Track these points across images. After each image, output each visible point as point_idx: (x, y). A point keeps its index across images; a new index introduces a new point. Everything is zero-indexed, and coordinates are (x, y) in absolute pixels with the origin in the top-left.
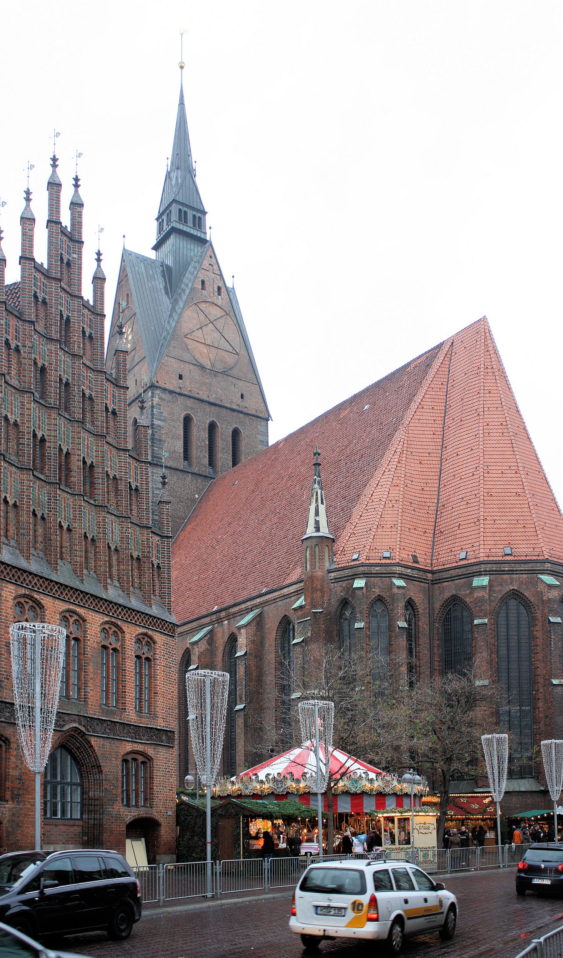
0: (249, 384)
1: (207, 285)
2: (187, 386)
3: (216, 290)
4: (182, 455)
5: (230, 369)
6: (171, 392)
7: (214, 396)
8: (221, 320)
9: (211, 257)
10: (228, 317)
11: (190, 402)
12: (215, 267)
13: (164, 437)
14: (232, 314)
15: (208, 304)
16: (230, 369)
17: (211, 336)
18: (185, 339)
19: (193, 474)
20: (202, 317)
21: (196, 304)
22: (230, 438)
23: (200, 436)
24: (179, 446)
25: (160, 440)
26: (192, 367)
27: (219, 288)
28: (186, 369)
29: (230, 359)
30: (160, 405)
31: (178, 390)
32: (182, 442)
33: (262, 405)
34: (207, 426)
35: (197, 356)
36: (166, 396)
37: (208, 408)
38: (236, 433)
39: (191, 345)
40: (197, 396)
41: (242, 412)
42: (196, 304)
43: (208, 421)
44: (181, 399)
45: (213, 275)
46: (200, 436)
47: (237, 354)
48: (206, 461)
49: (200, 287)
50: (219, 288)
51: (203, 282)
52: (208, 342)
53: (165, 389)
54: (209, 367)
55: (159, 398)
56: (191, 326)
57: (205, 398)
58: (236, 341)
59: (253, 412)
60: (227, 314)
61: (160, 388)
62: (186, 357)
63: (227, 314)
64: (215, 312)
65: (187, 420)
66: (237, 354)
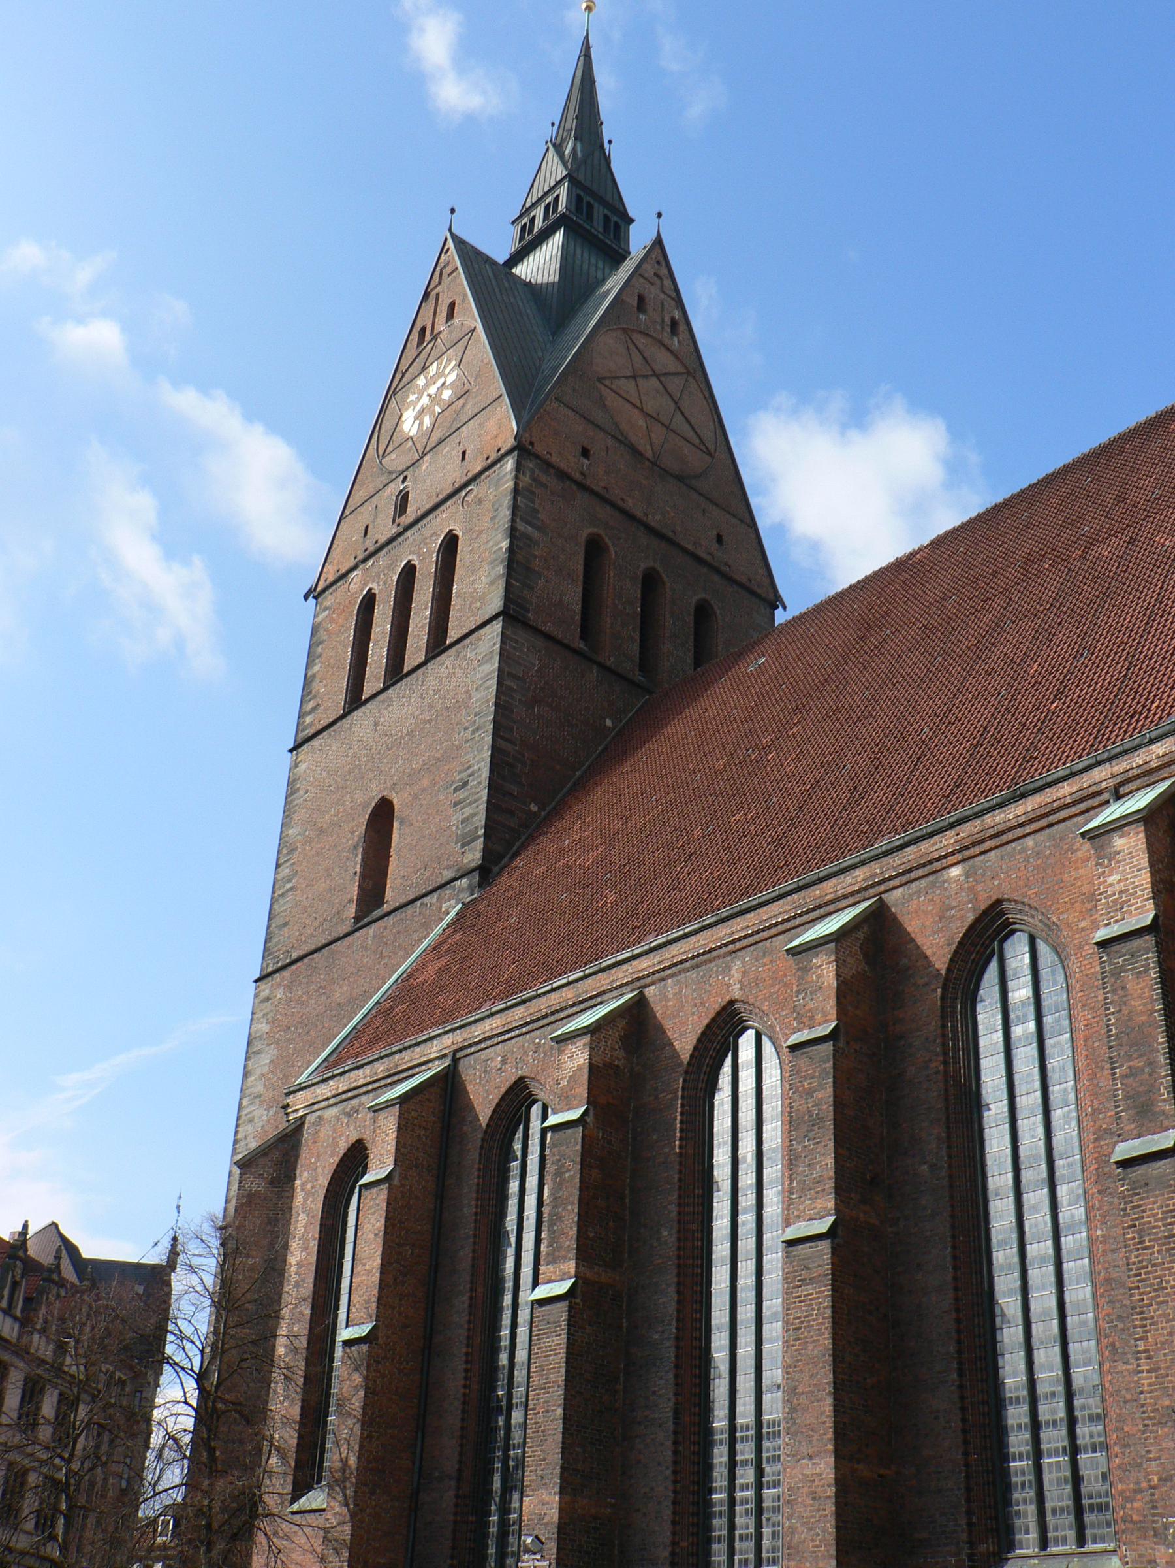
0: (734, 521)
1: (650, 309)
3: (667, 320)
4: (578, 618)
6: (562, 475)
7: (658, 517)
9: (658, 263)
10: (691, 379)
12: (667, 282)
13: (536, 564)
14: (699, 375)
15: (650, 340)
17: (657, 403)
18: (597, 383)
19: (602, 667)
20: (637, 359)
21: (624, 330)
22: (692, 618)
23: (621, 591)
24: (573, 595)
25: (528, 569)
26: (610, 442)
27: (674, 324)
29: (695, 460)
30: (533, 493)
31: (578, 476)
32: (580, 589)
33: (762, 571)
34: (640, 574)
38: (703, 612)
39: (611, 399)
40: (619, 502)
41: (717, 571)
42: (624, 330)
43: (643, 566)
45: (662, 296)
46: (621, 591)
47: (709, 454)
48: (634, 649)
49: (635, 304)
50: (674, 324)
51: (641, 299)
52: (649, 408)
53: (548, 465)
55: (534, 479)
57: (639, 514)
58: (708, 434)
59: (744, 580)
60: (688, 373)
61: (537, 457)
63: (688, 373)
64: (664, 361)
65: (594, 549)
66: (709, 454)
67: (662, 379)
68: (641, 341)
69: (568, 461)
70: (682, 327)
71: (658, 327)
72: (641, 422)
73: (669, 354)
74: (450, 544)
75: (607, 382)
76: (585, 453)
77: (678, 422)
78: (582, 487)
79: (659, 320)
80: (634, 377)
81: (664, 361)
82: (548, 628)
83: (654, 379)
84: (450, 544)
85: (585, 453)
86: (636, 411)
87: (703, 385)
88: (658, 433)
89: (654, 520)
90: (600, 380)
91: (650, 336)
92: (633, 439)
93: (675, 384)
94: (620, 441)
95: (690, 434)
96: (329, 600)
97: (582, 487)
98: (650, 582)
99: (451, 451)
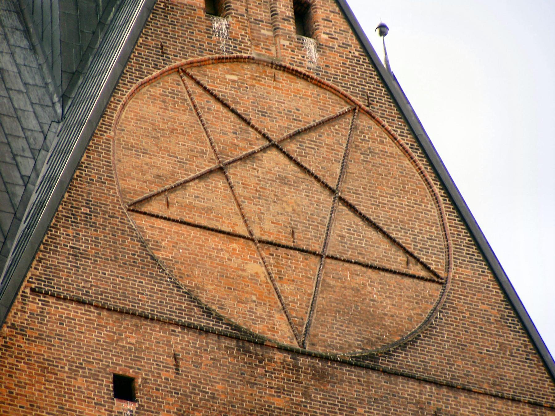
5: (403, 346)
8: (327, 136)
10: (364, 122)
14: (382, 106)
15: (248, 70)
16: (403, 346)
20: (224, 125)
21: (181, 71)
26: (182, 341)
29: (398, 304)
35: (211, 293)
42: (181, 71)
47: (435, 278)
52: (267, 229)
54: (283, 335)
56: (164, 164)
60: (355, 109)
62: (147, 294)
63: (355, 109)
64: (288, 104)
66: (435, 278)
67: (291, 147)
68: (222, 79)
71: (266, 32)
72: (255, 268)
73: (301, 84)
75: (154, 207)
79: (264, 15)
80: (221, 170)
81: (288, 104)
83: (273, 154)
86: (236, 245)
87: (397, 127)
91: (249, 60)
92: (238, 314)
93: (322, 153)
94: (207, 331)
95: (380, 251)
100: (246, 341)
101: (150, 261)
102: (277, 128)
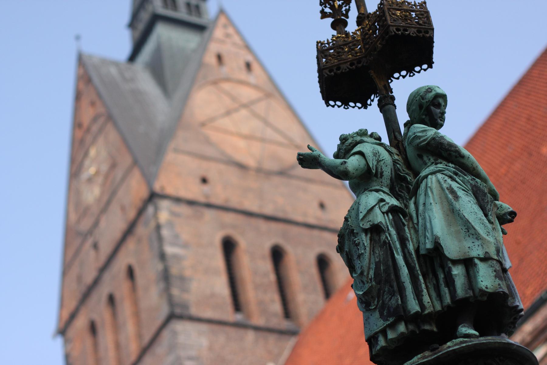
2: (218, 193)
6: (191, 203)
11: (229, 218)
13: (188, 273)
19: (257, 329)
20: (227, 101)
26: (222, 167)
27: (248, 66)
28: (213, 171)
36: (184, 209)
37: (263, 225)
39: (214, 136)
44: (209, 214)
48: (277, 307)
50: (248, 66)
51: (219, 58)
62: (209, 151)
65: (229, 246)
68: (226, 86)
69: (195, 191)
70: (255, 66)
74: (131, 273)
76: (204, 181)
77: (269, 133)
78: (209, 206)
82: (208, 314)
84: (131, 273)
85: (204, 181)
88: (256, 148)
89: (269, 210)
90: (203, 124)
93: (260, 108)
96: (71, 333)
97: (209, 206)
98: (277, 255)
99: (115, 208)
100: (242, 167)
101: (207, 141)
102: (245, 101)
